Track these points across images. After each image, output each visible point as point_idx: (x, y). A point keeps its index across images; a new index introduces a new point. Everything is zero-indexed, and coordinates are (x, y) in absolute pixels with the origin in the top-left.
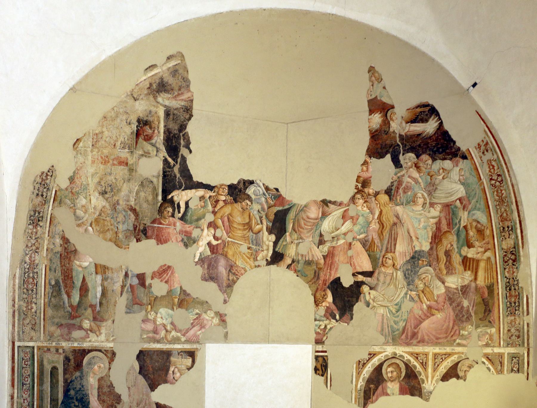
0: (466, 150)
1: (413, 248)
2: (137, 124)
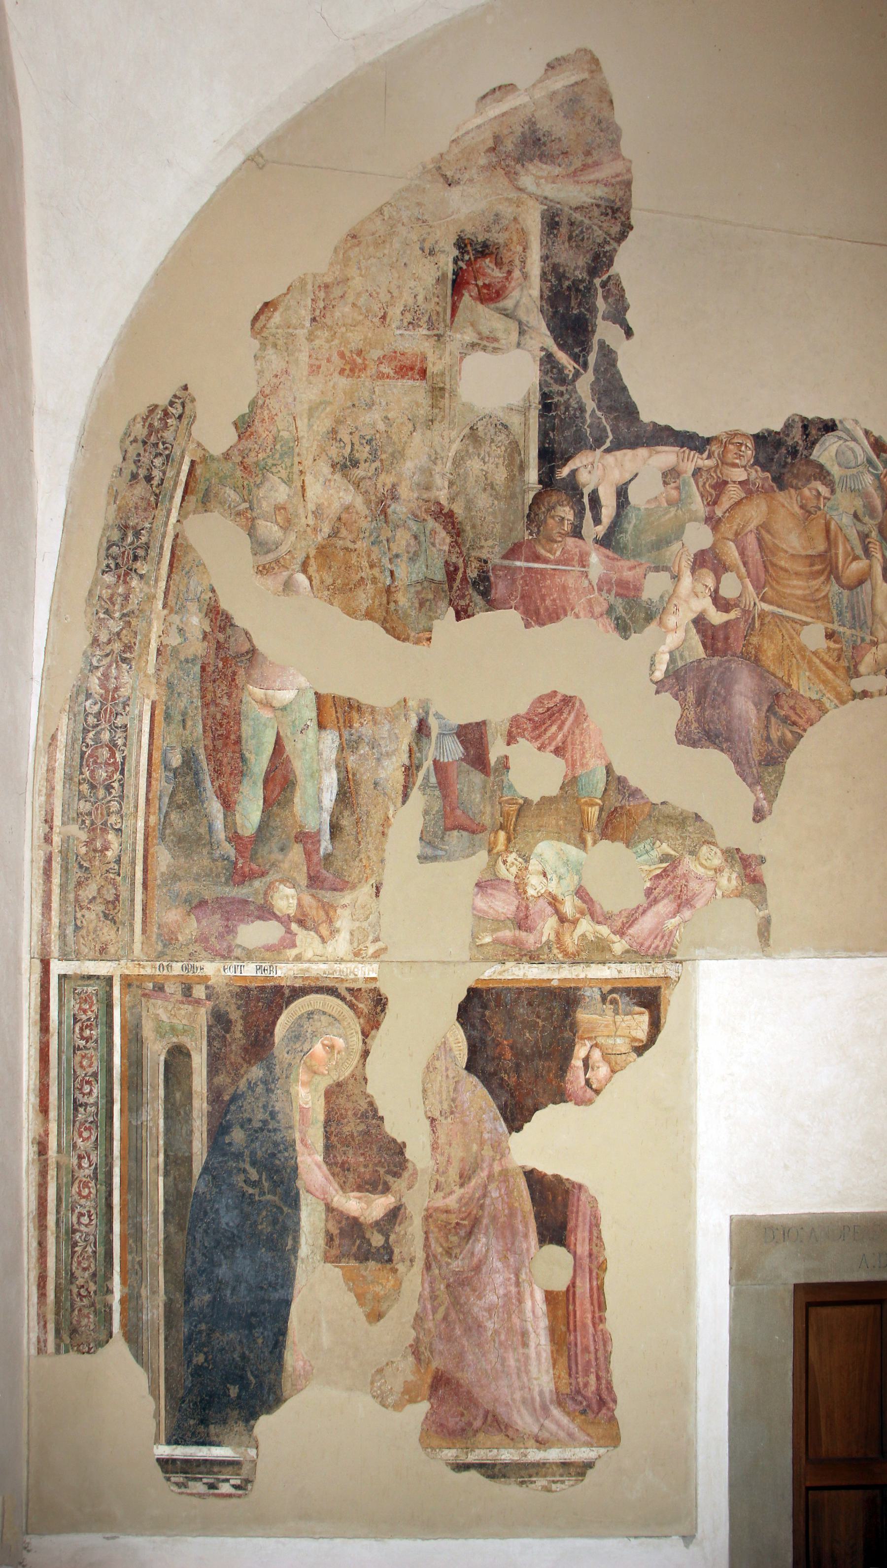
2: (456, 252)
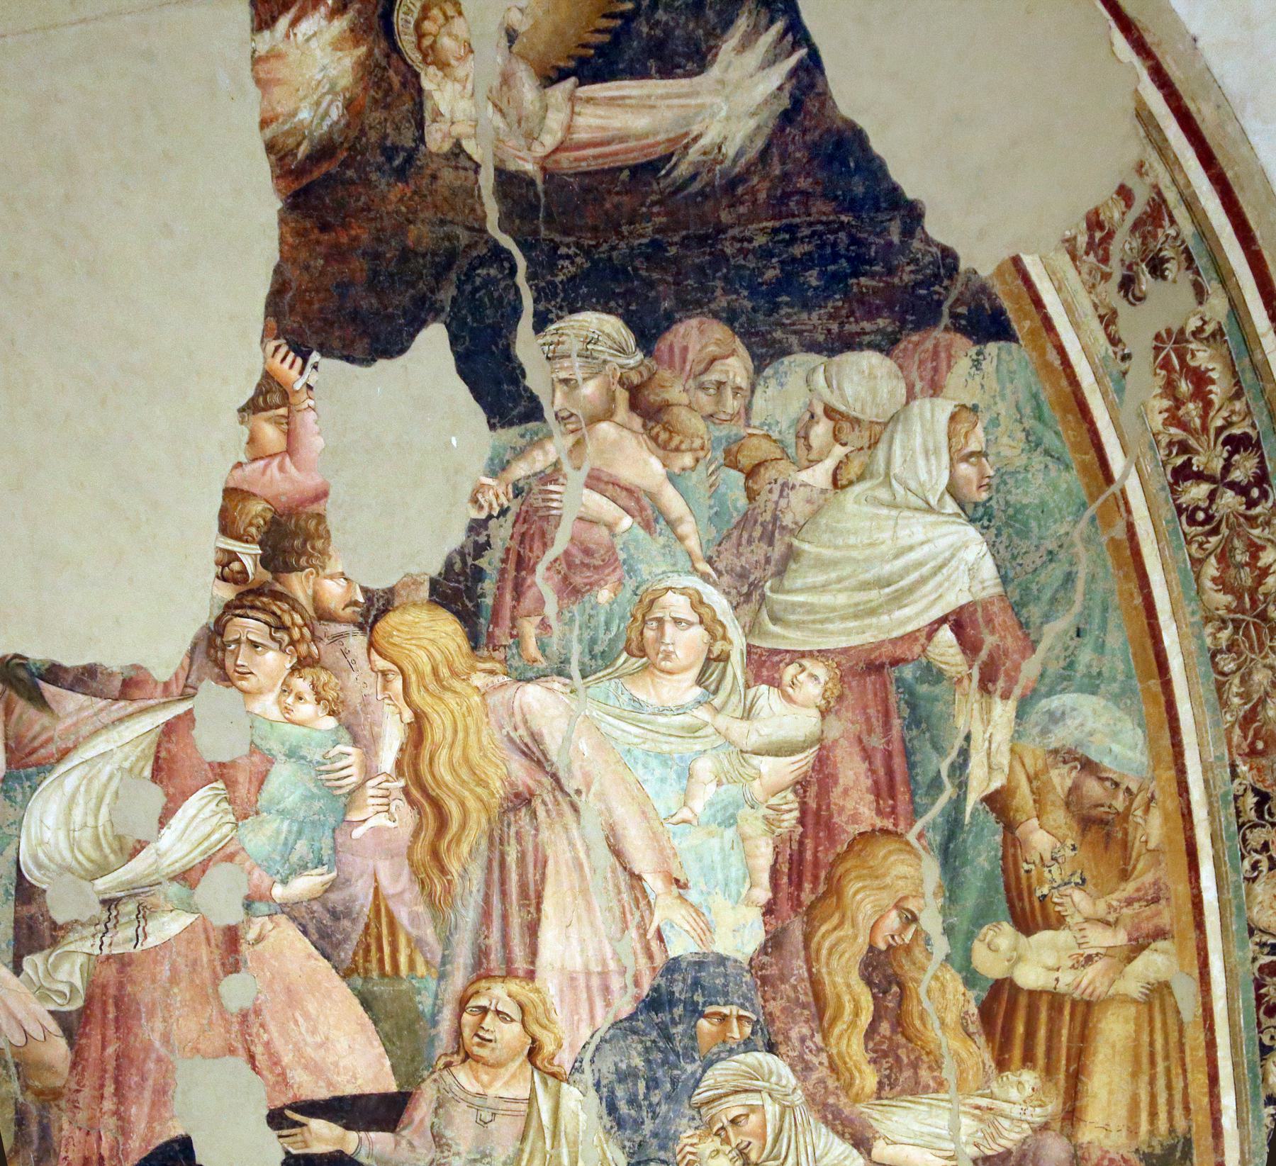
0: (1000, 272)
1: (655, 945)
